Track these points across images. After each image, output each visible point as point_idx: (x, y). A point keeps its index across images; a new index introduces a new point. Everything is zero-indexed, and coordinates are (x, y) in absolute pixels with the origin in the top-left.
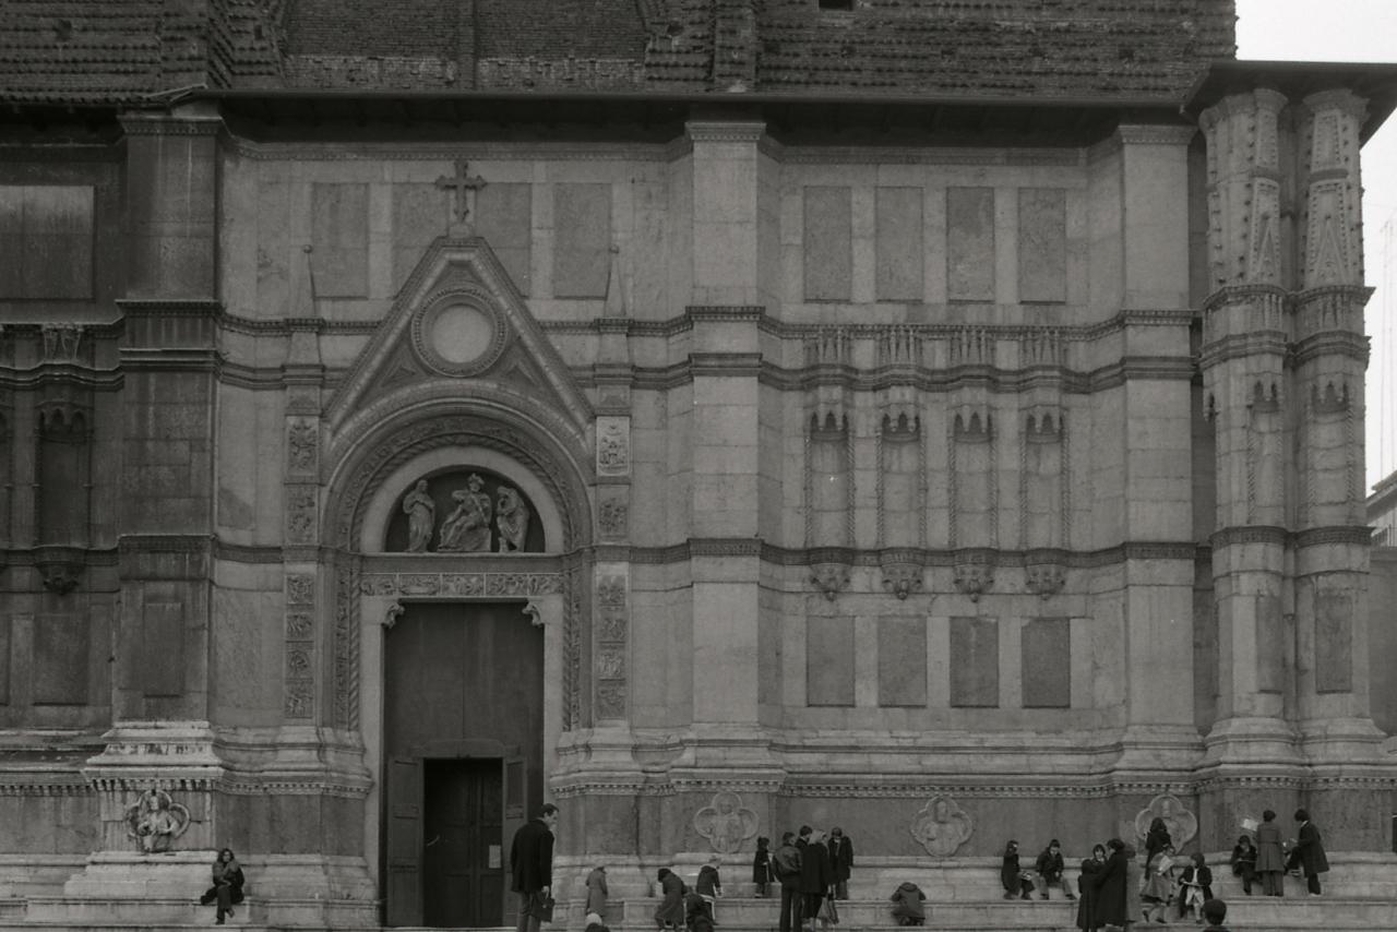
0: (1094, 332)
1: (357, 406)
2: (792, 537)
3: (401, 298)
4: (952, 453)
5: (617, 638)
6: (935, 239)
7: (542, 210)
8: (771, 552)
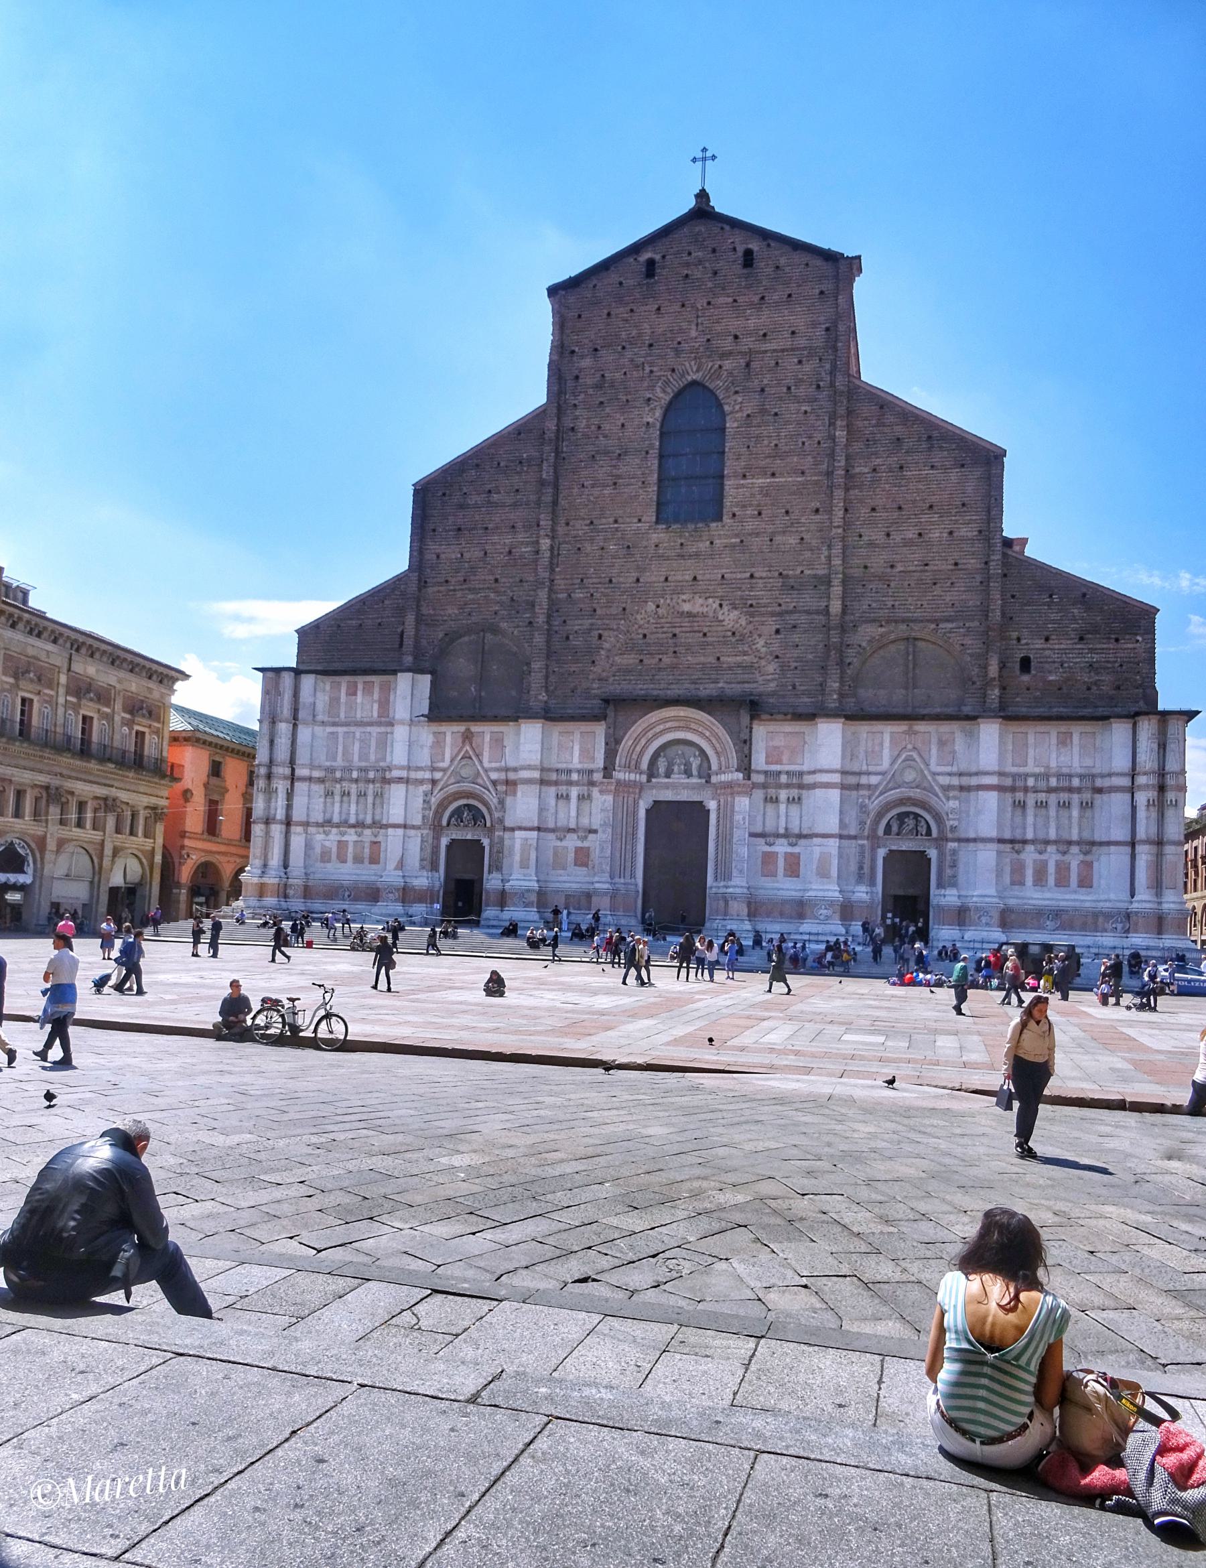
0: (1103, 776)
1: (879, 796)
2: (1007, 835)
3: (892, 763)
4: (1057, 811)
5: (954, 865)
6: (1054, 748)
7: (934, 740)
8: (1001, 841)
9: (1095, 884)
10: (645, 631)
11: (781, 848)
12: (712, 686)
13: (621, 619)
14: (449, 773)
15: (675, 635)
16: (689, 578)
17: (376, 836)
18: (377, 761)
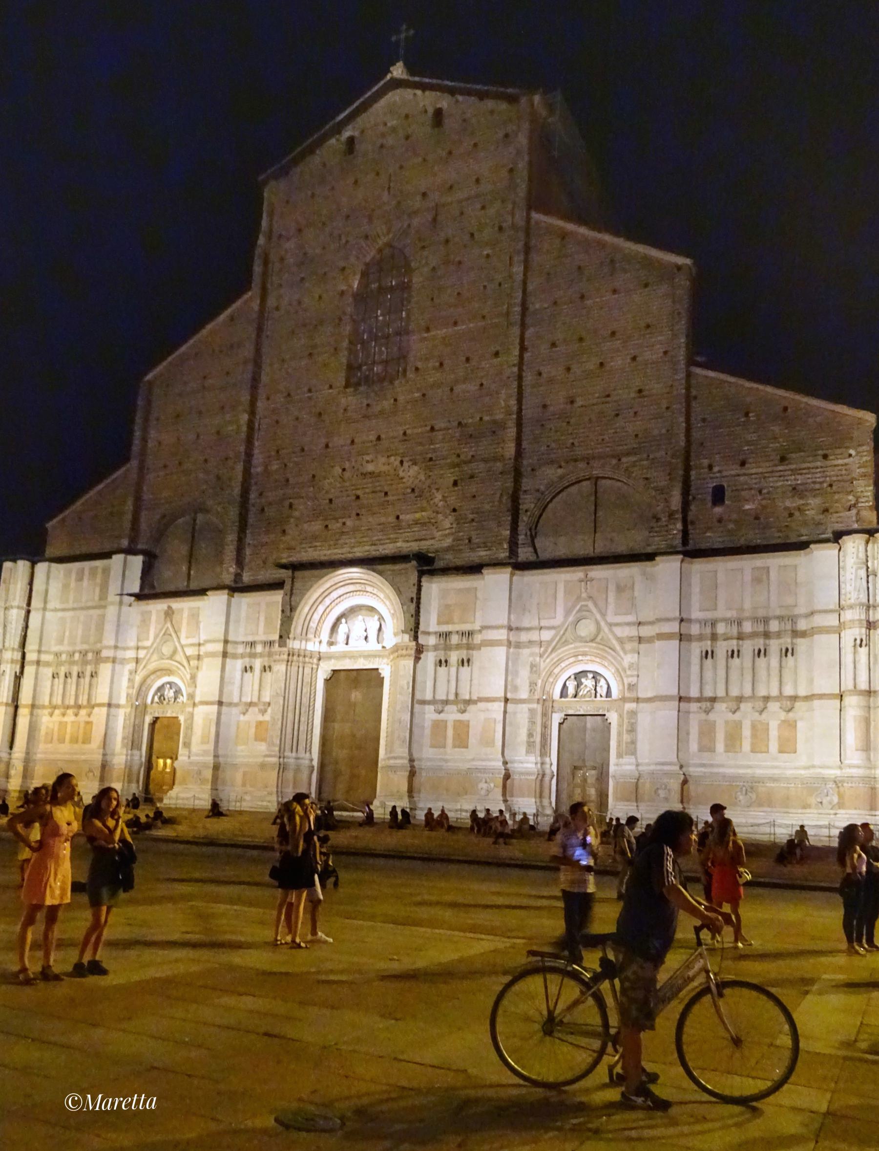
9: (800, 746)
10: (331, 496)
11: (451, 715)
12: (391, 546)
13: (310, 487)
14: (151, 651)
15: (358, 497)
16: (373, 437)
17: (89, 715)
18: (95, 643)
